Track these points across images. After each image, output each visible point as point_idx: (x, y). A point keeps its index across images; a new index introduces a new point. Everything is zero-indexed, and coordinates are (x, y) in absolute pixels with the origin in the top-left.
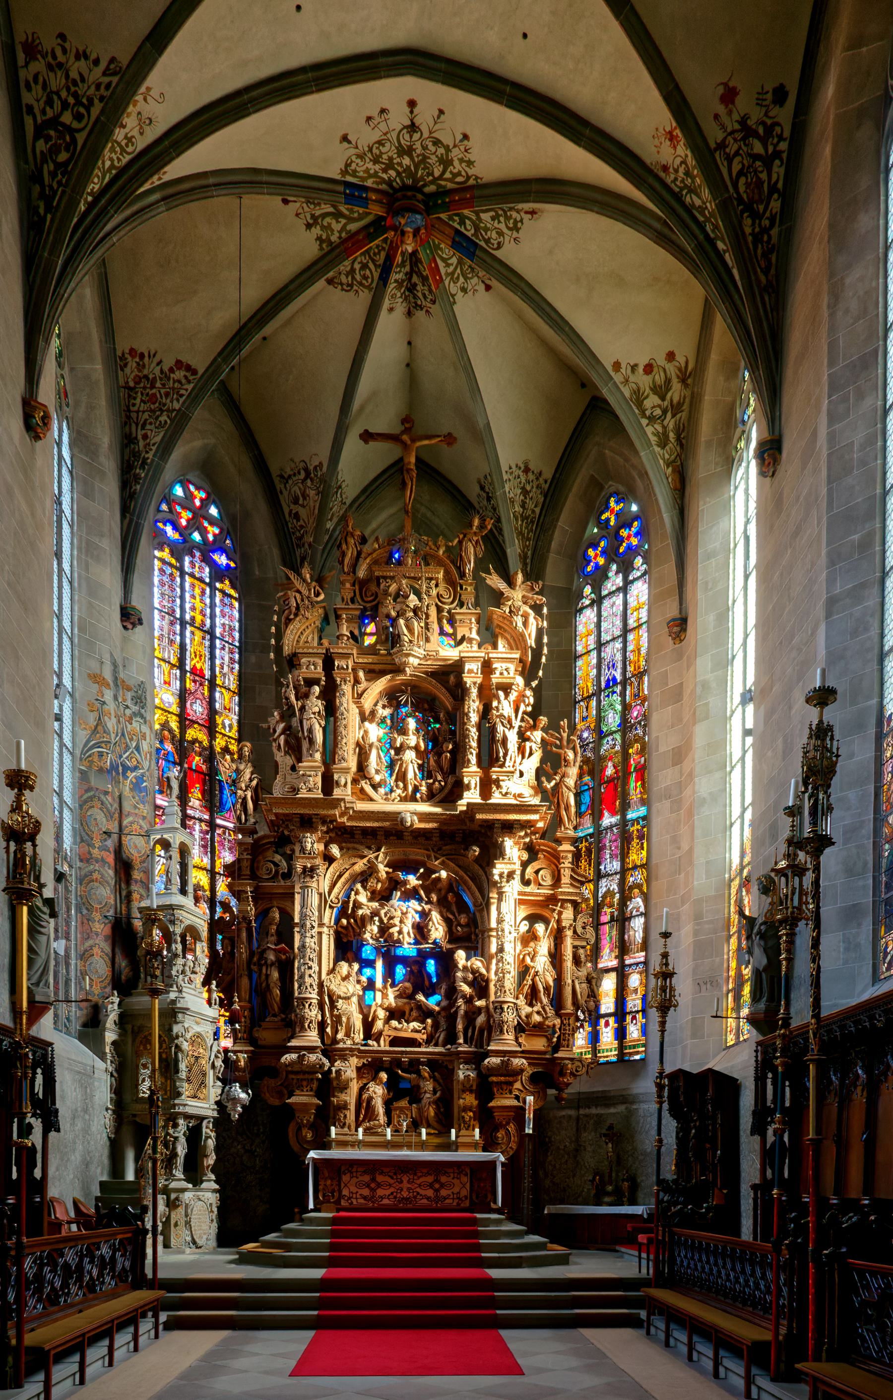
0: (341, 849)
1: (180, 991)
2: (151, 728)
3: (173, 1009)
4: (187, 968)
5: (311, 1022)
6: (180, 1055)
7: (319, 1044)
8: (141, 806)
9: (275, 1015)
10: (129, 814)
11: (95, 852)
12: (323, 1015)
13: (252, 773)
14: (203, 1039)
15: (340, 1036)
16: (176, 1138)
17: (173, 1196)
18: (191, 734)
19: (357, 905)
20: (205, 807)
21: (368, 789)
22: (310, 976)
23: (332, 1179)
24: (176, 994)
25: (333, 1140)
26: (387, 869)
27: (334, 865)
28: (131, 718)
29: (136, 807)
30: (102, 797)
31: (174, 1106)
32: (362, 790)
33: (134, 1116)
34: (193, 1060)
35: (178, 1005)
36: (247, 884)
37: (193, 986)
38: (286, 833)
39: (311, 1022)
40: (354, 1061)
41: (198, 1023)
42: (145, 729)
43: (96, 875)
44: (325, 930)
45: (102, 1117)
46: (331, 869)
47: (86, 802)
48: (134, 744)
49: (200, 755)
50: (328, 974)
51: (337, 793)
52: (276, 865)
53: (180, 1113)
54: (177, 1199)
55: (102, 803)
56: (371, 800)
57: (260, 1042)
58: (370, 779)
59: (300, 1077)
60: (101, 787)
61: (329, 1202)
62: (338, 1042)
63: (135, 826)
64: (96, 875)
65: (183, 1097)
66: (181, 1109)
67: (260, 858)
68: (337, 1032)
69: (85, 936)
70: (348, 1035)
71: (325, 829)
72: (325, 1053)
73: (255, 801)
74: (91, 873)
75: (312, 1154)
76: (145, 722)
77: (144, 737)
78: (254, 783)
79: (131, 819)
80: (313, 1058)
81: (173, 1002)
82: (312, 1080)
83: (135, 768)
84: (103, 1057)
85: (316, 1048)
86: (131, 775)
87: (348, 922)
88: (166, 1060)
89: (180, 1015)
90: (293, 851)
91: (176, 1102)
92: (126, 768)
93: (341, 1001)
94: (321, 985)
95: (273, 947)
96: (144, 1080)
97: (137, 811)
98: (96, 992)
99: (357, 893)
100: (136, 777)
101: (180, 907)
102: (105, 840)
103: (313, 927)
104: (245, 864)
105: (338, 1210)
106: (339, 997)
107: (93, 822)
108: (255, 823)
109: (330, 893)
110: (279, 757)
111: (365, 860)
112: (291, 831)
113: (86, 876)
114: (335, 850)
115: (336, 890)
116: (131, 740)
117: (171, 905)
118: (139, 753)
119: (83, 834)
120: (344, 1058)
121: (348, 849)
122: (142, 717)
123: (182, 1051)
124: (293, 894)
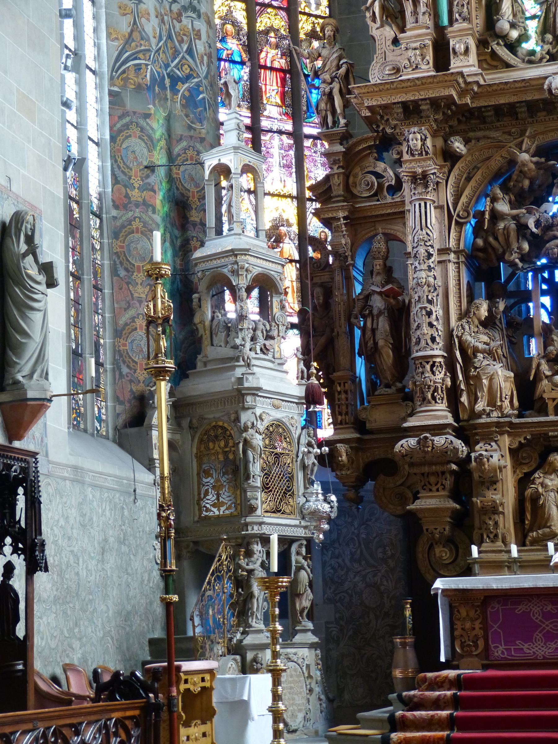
0: (467, 142)
1: (248, 365)
2: (210, 23)
3: (239, 391)
4: (259, 333)
5: (436, 390)
6: (250, 454)
7: (450, 420)
8: (197, 126)
9: (388, 386)
10: (180, 139)
11: (135, 194)
12: (454, 378)
13: (340, 58)
14: (286, 429)
15: (480, 406)
16: (251, 572)
17: (250, 656)
18: (263, 22)
19: (496, 216)
20: (286, 114)
21: (503, 52)
22: (431, 325)
23: (473, 620)
24: (243, 370)
25: (475, 561)
26: (535, 159)
27: (459, 165)
28: (180, 15)
29: (190, 128)
30: (142, 122)
31: (246, 525)
32: (494, 54)
33: (196, 543)
34: (271, 459)
35: (246, 385)
36: (337, 209)
37: (270, 357)
38: (389, 131)
39: (436, 390)
40: (506, 441)
41: (276, 407)
42: (201, 25)
43: (136, 224)
44: (452, 256)
45: (150, 549)
46: (455, 172)
47: (120, 131)
48: (185, 47)
49: (277, 47)
50: (460, 319)
51: (456, 64)
52: (378, 176)
53: (254, 536)
54: (255, 660)
55: (142, 129)
56: (508, 66)
57: (368, 426)
58: (504, 37)
59: (426, 469)
60: (140, 109)
61: (470, 655)
62: (479, 415)
63: (190, 153)
64: (136, 224)
65: (259, 512)
66: (256, 530)
67: (357, 170)
68: (476, 399)
69: (123, 304)
70: (492, 403)
71: (440, 117)
72: (460, 433)
73: (345, 92)
74: (130, 222)
75: (439, 584)
76: (199, 16)
77: (198, 35)
78: (343, 70)
79: (184, 144)
80: (440, 441)
81: (240, 380)
82: (443, 473)
83: (188, 77)
84: (150, 466)
85: (445, 426)
86: (183, 88)
87: (486, 241)
88: (234, 461)
89: (249, 398)
90: (400, 153)
91: (249, 519)
92: (175, 80)
93: (480, 356)
94: (449, 335)
95: (378, 290)
96: (206, 493)
97: (192, 133)
98: (141, 378)
99: (494, 200)
100: (189, 90)
101: (245, 252)
102: (148, 177)
103: (430, 256)
104: (336, 181)
105: (485, 667)
106: (476, 350)
107: (131, 157)
108: (346, 125)
109: (455, 205)
110: (375, 30)
111: (504, 153)
112: (395, 128)
113: (123, 226)
114: (458, 145)
115: (464, 199)
116: (181, 42)
117: (232, 251)
118: (192, 57)
119: (117, 172)
120: (488, 438)
121: (478, 139)
122: (195, 10)
123: (253, 448)
124: (403, 212)
